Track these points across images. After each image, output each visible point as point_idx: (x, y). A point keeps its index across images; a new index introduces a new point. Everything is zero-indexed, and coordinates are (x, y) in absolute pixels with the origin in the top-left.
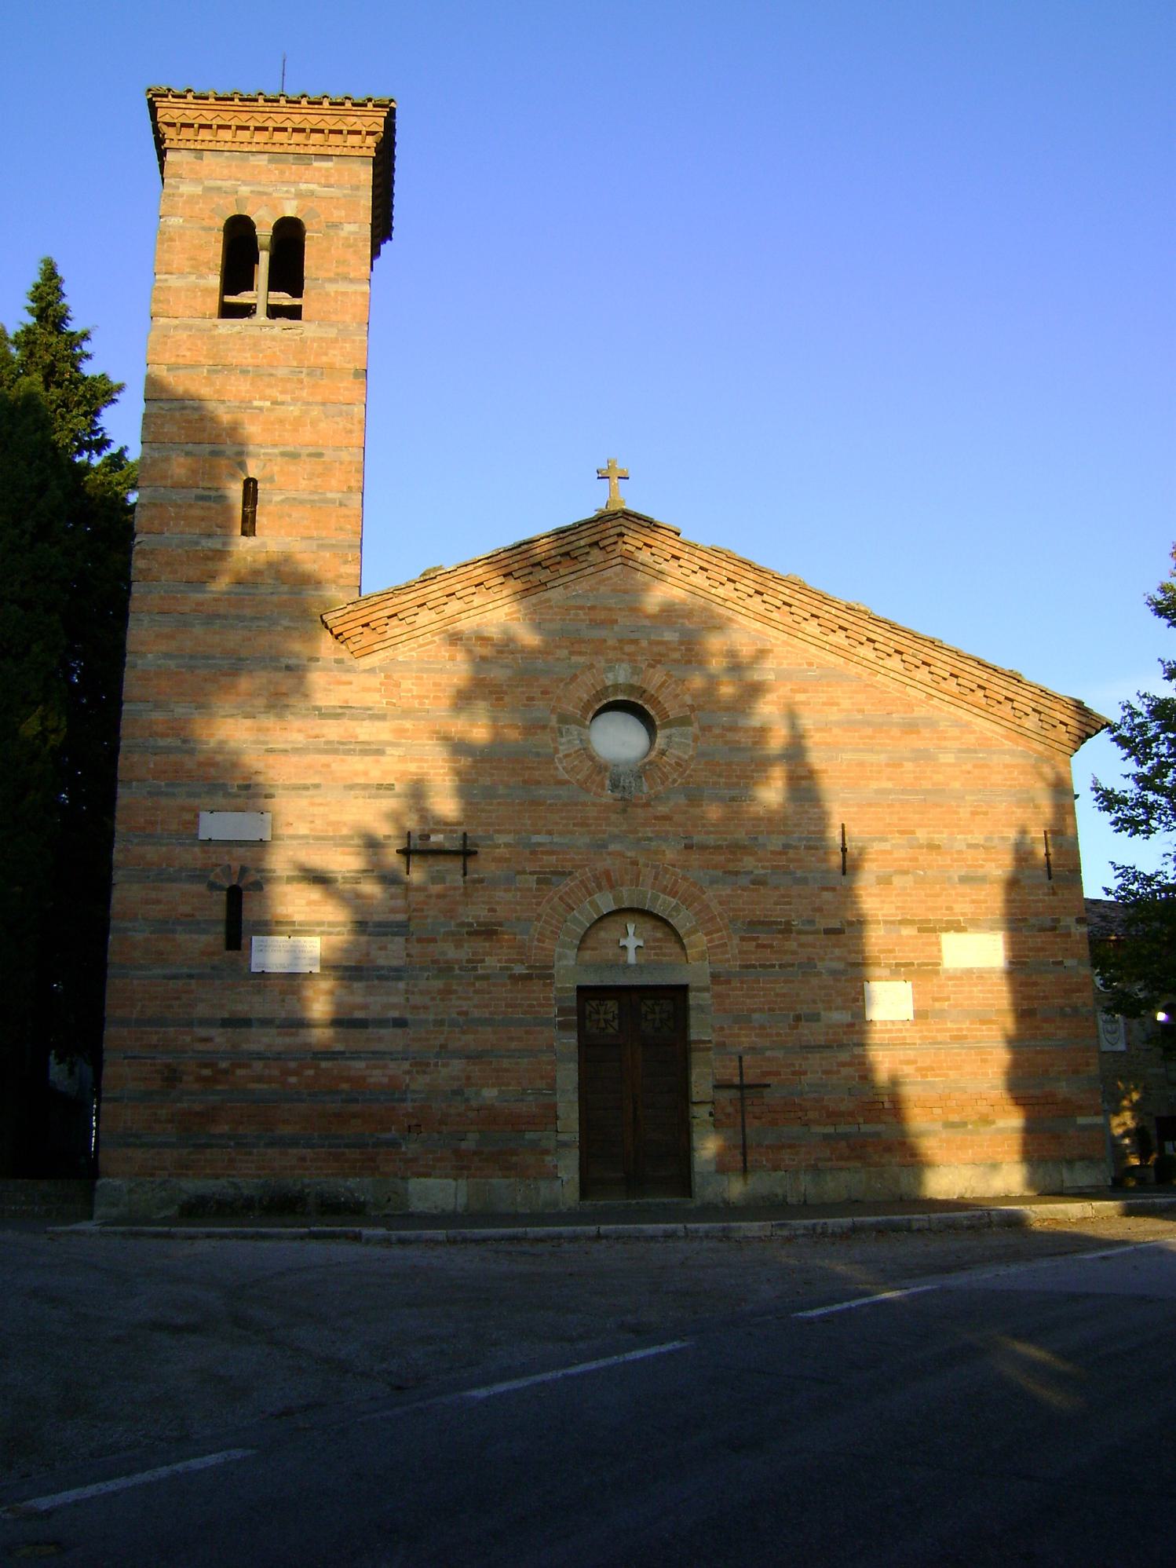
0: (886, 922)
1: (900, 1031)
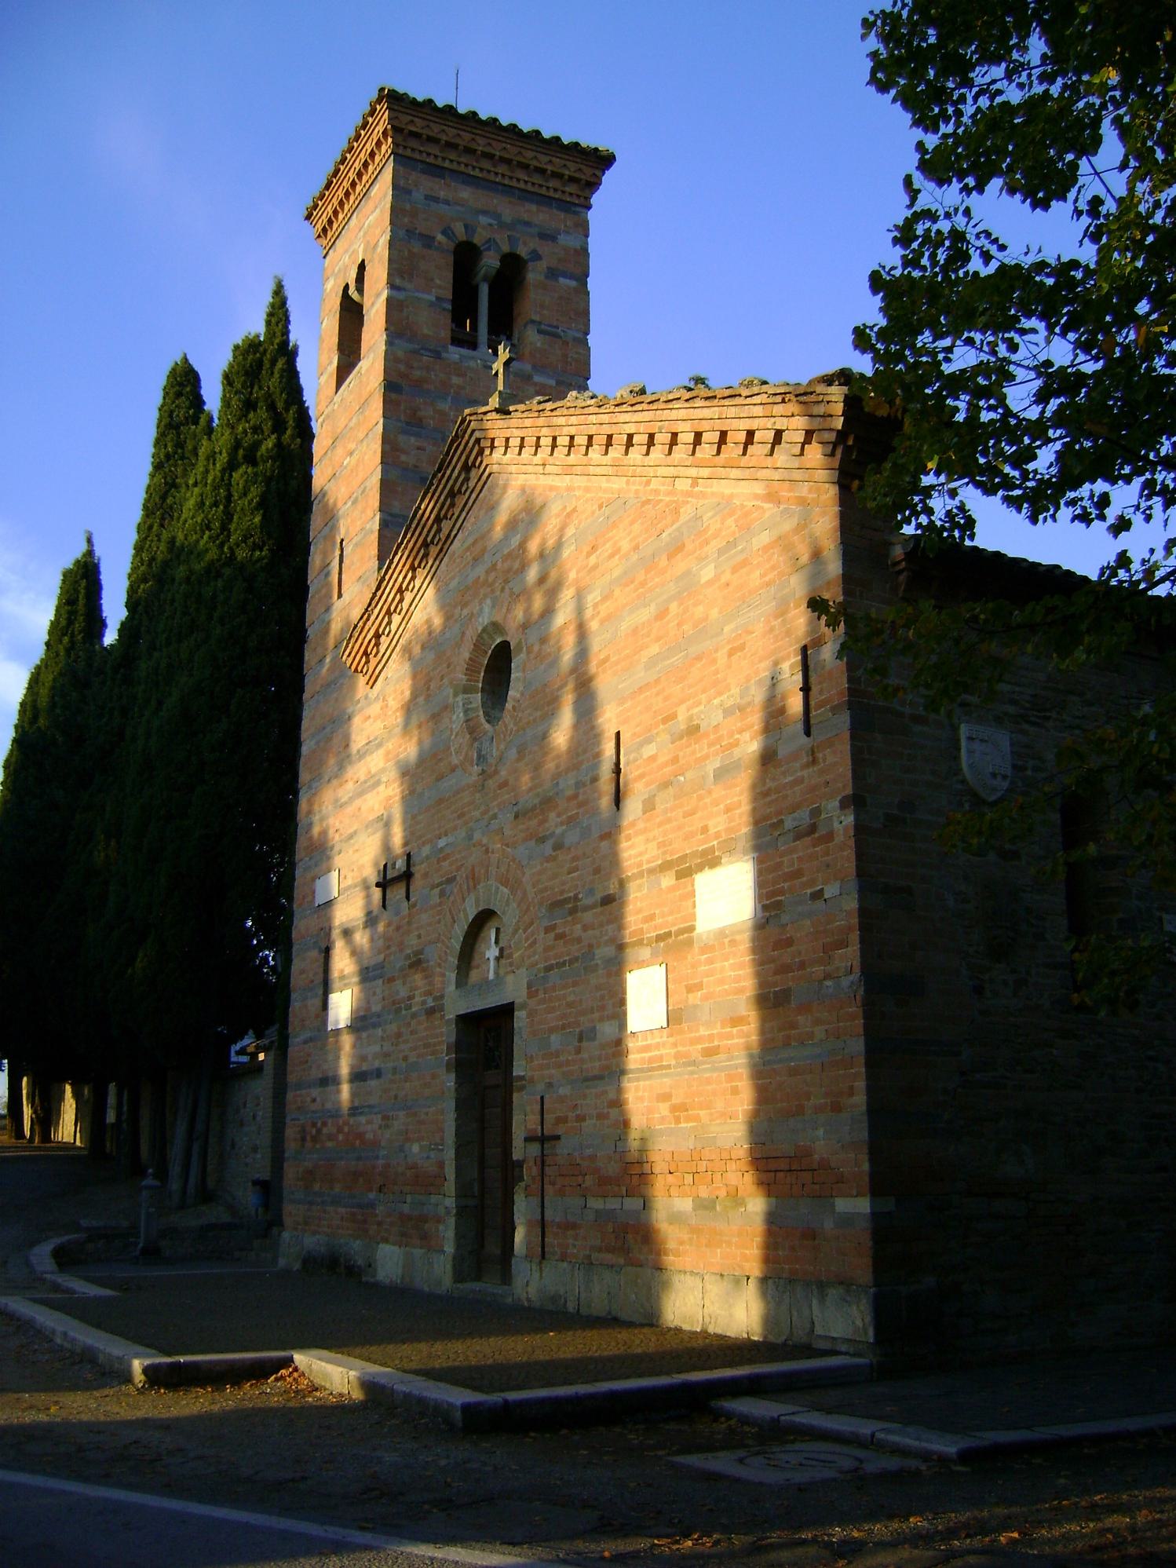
0: (651, 871)
1: (657, 1046)
